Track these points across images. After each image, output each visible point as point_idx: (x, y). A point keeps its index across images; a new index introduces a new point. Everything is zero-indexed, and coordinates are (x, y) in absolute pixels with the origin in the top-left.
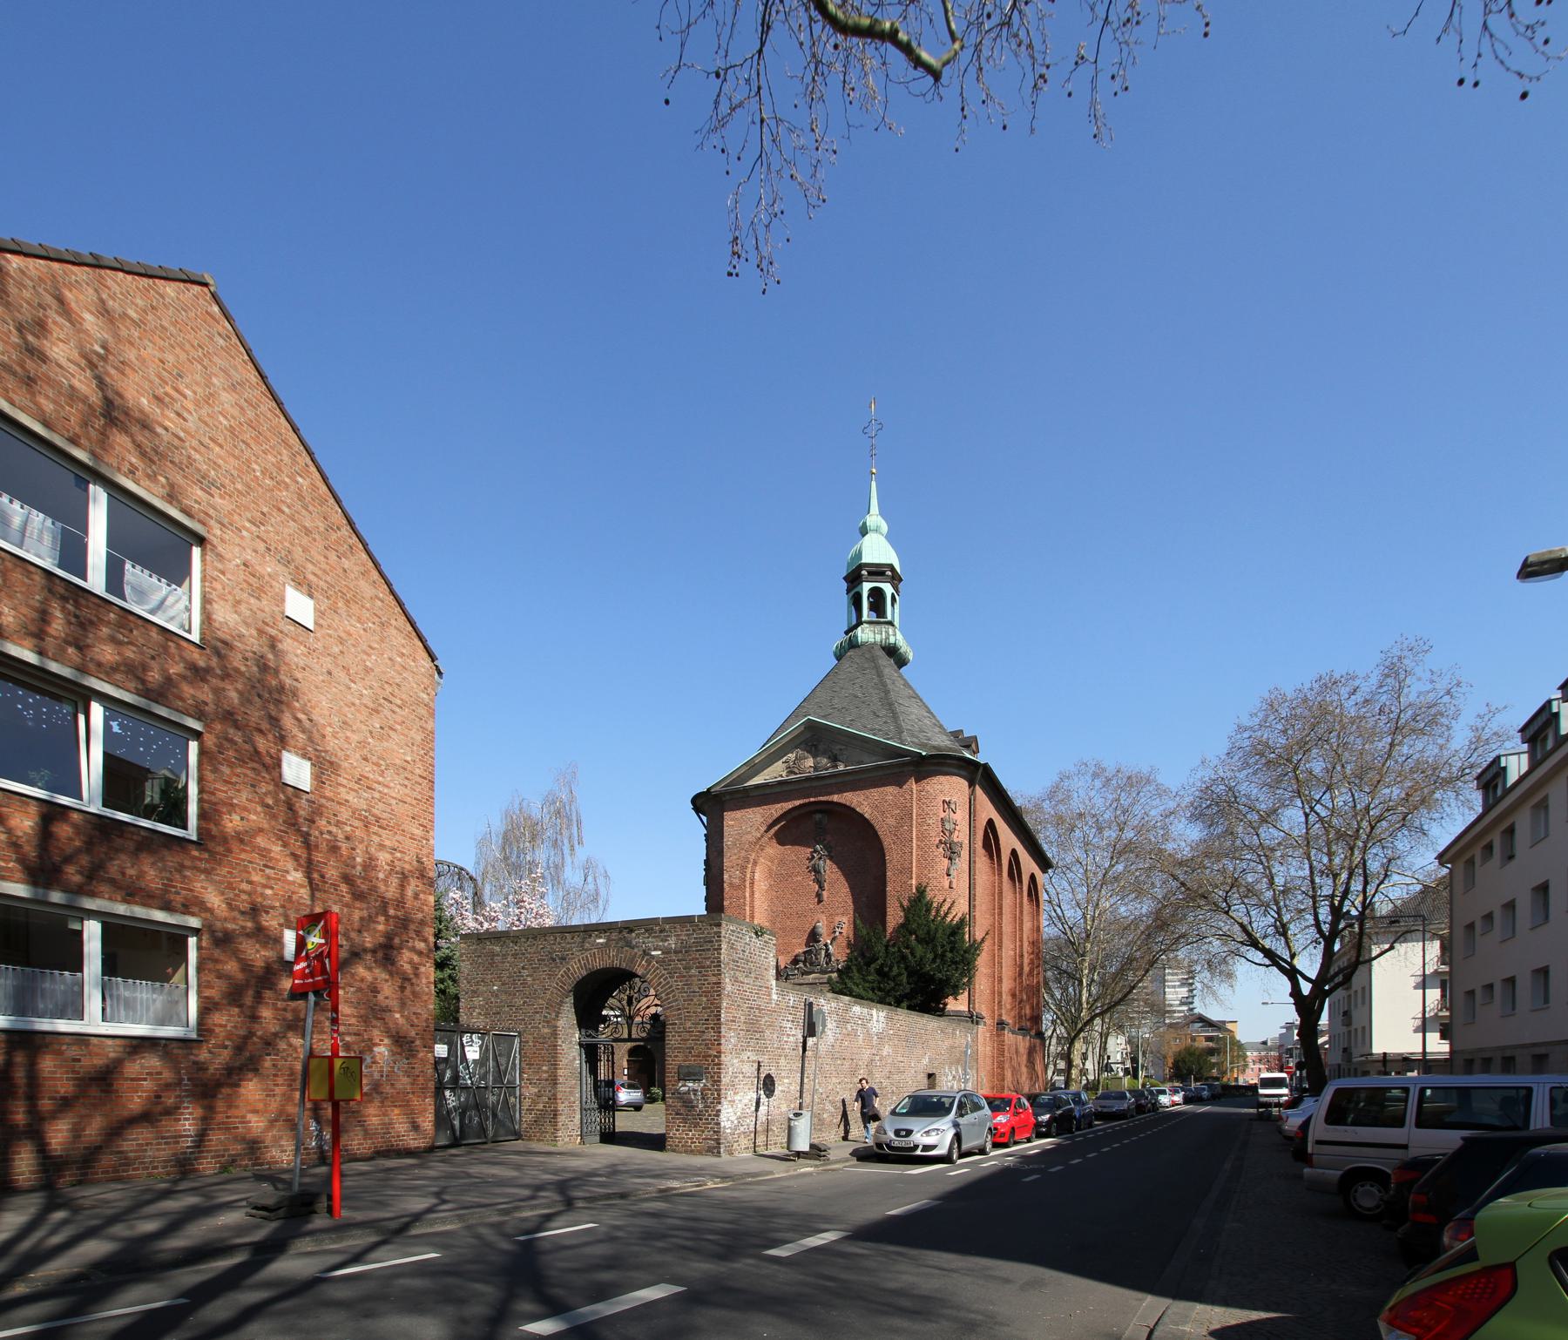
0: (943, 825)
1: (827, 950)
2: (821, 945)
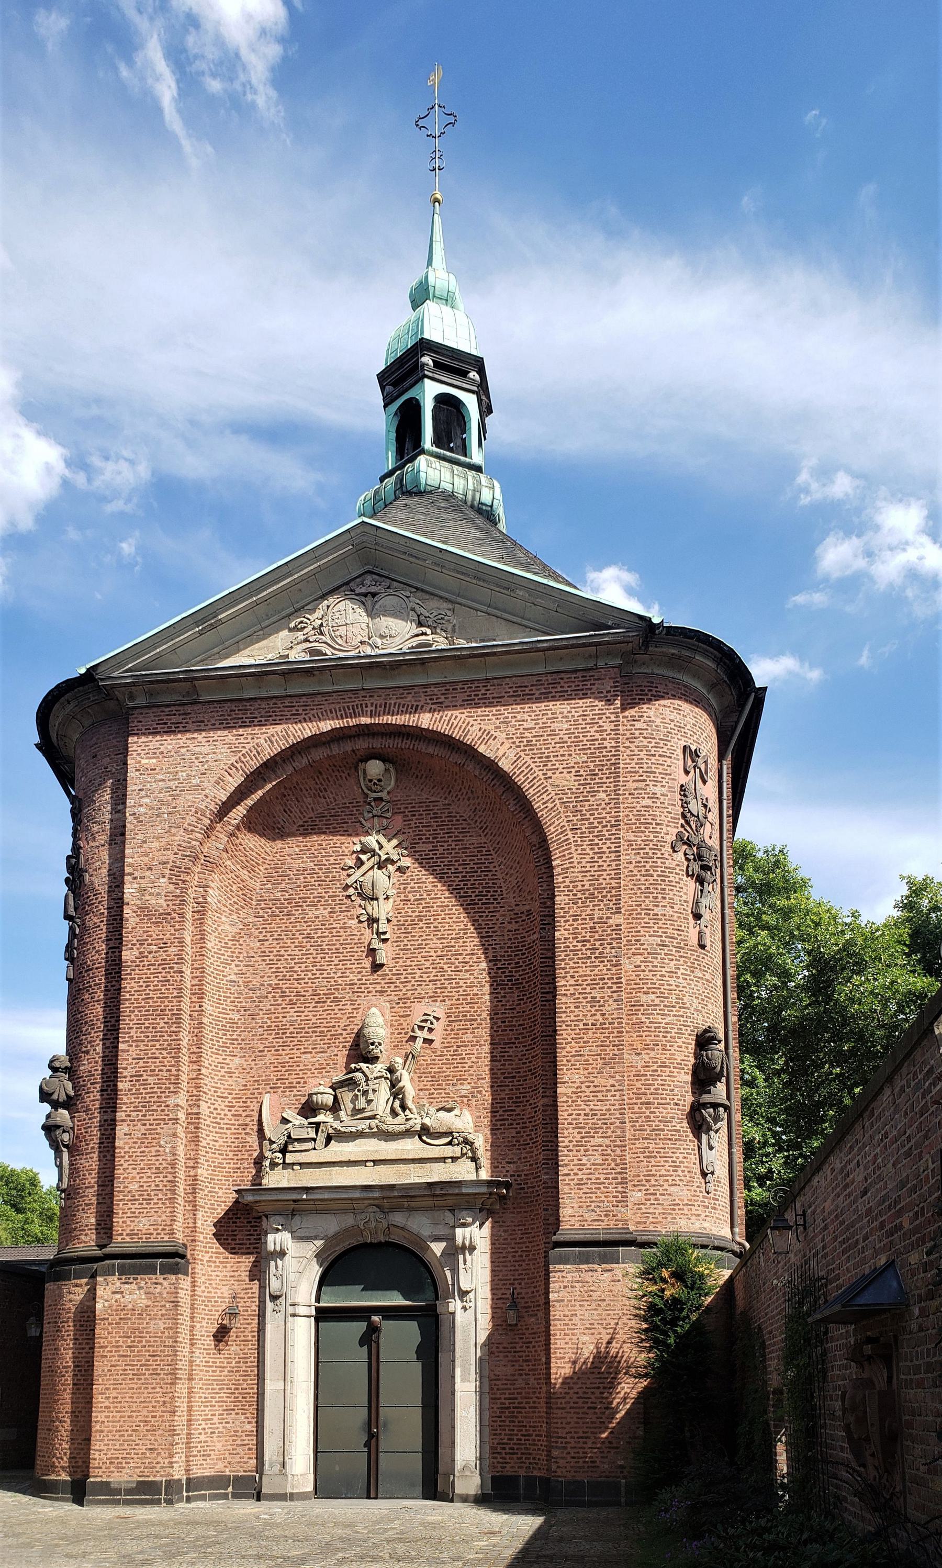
0: (684, 805)
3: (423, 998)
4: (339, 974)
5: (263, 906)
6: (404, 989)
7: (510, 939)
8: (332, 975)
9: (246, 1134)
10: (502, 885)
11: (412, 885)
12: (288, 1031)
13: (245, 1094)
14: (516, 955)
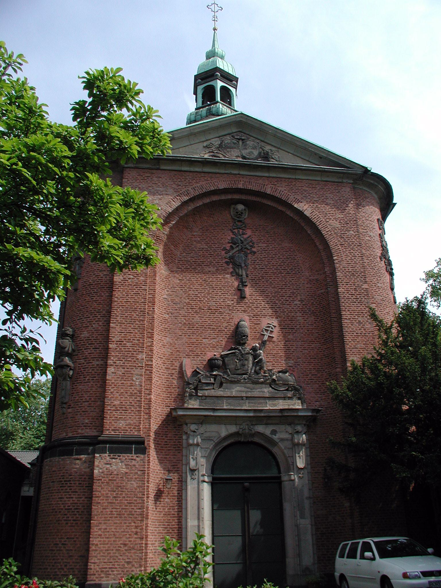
1: (255, 357)
2: (248, 348)
3: (266, 316)
4: (222, 300)
5: (181, 263)
6: (256, 311)
7: (308, 291)
8: (218, 300)
9: (173, 378)
10: (302, 266)
11: (257, 261)
12: (195, 327)
13: (172, 357)
14: (312, 299)
